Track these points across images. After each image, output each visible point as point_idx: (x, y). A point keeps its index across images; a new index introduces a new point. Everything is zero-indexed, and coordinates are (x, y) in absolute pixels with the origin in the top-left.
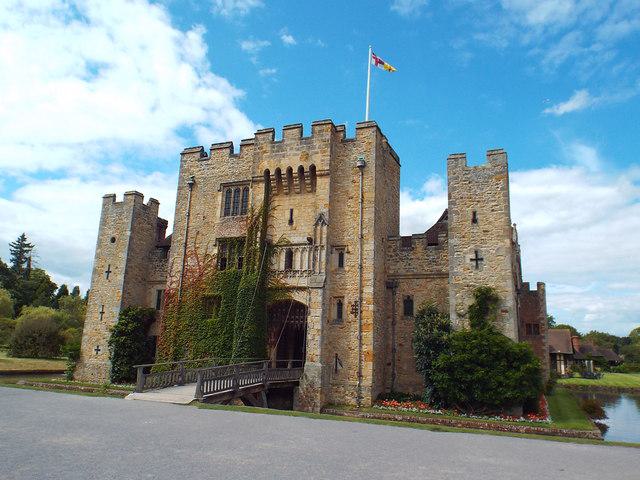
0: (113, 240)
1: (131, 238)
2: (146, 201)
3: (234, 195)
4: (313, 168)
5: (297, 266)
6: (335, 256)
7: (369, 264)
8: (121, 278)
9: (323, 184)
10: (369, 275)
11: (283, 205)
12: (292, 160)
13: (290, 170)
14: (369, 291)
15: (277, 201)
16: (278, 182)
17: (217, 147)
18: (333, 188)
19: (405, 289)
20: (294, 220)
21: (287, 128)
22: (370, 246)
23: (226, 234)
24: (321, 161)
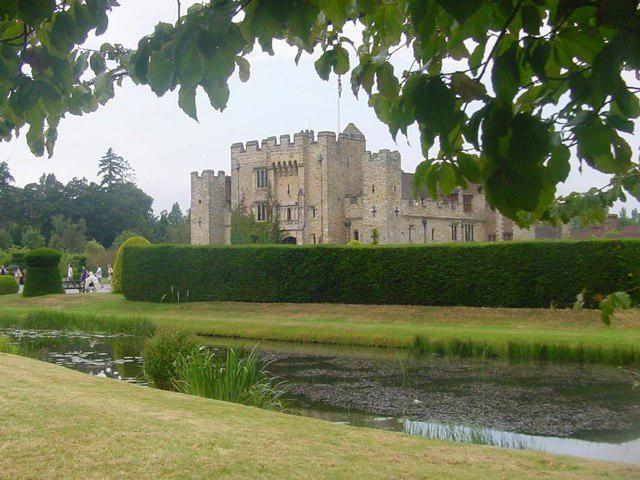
0: (200, 202)
1: (210, 201)
2: (216, 175)
3: (261, 173)
4: (295, 162)
5: (293, 218)
6: (311, 212)
7: (325, 216)
8: (207, 225)
9: (301, 171)
10: (326, 222)
11: (284, 181)
12: (285, 158)
13: (285, 163)
14: (326, 230)
15: (280, 181)
16: (281, 169)
17: (250, 144)
18: (306, 173)
19: (355, 226)
20: (286, 192)
21: (282, 137)
22: (326, 206)
23: (258, 199)
24: (298, 158)
